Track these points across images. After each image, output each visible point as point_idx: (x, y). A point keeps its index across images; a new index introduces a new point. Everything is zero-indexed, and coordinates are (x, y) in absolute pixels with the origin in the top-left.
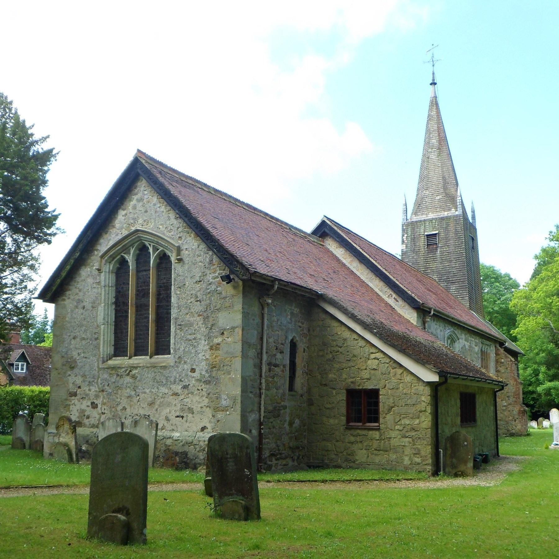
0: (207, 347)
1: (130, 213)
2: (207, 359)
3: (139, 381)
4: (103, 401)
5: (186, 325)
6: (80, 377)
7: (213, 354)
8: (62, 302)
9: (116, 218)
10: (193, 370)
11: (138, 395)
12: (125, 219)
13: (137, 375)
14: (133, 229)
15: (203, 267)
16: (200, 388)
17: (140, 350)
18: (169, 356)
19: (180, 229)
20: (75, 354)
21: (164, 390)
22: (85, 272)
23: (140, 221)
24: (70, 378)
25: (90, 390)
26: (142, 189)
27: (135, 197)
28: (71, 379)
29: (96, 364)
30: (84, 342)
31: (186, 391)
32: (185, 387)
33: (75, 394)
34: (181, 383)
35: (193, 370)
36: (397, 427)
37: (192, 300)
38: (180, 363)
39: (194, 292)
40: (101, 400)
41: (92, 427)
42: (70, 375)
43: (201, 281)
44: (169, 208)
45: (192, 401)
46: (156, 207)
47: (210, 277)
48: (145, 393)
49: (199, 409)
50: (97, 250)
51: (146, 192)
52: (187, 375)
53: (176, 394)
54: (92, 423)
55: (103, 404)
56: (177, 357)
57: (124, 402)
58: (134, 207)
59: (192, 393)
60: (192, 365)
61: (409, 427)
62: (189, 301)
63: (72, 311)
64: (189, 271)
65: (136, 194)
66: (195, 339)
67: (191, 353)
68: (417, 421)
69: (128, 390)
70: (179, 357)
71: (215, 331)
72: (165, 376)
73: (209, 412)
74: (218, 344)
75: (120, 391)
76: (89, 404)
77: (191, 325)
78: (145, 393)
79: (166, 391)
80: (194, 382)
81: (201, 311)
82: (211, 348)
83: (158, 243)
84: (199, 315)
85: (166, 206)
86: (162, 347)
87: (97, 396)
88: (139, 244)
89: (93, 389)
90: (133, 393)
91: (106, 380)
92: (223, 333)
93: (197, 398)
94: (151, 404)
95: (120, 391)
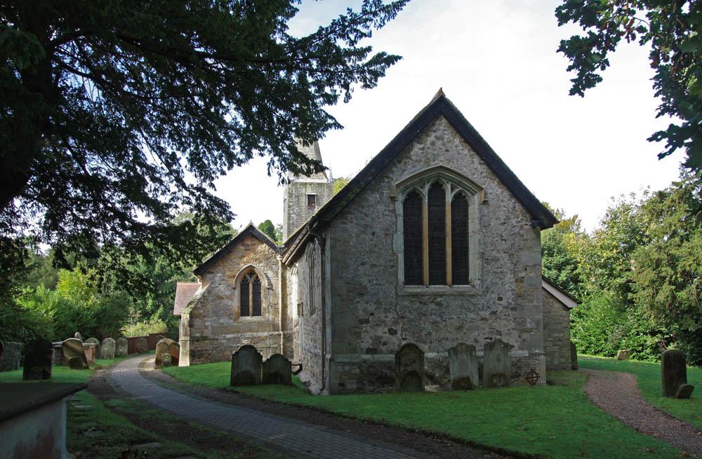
0: (513, 280)
1: (429, 148)
2: (513, 290)
3: (445, 308)
4: (402, 328)
5: (492, 260)
6: (372, 304)
7: (518, 286)
8: (343, 226)
9: (411, 150)
10: (500, 299)
11: (445, 321)
12: (423, 153)
13: (443, 302)
14: (433, 165)
15: (507, 212)
16: (507, 314)
17: (437, 278)
18: (401, 277)
19: (484, 175)
20: (365, 281)
21: (472, 316)
22: (373, 198)
23: (442, 158)
24: (359, 305)
25: (386, 317)
26: (442, 128)
27: (433, 135)
28: (361, 306)
29: (393, 291)
30: (376, 269)
31: (494, 317)
32: (494, 313)
33: (367, 321)
34: (489, 309)
35: (500, 299)
36: (550, 339)
37: (497, 238)
38: (487, 292)
39: (499, 232)
40: (401, 326)
41: (390, 353)
42: (358, 302)
43: (504, 223)
44: (472, 153)
45: (500, 324)
46: (458, 149)
47: (514, 221)
48: (452, 318)
49: (507, 331)
50: (388, 177)
51: (446, 132)
52: (494, 303)
53: (484, 319)
54: (390, 349)
55: (403, 330)
56: (485, 287)
57: (428, 327)
58: (433, 144)
59: (500, 318)
60: (499, 294)
61: (557, 339)
62: (495, 240)
63: (357, 236)
64: (495, 213)
65: (435, 132)
66: (501, 272)
67: (497, 284)
68: (562, 335)
69: (433, 317)
70: (487, 287)
71: (520, 266)
72: (472, 304)
73: (516, 334)
74: (523, 278)
75: (423, 318)
76: (386, 330)
77: (497, 260)
78: (452, 318)
79: (475, 317)
80: (501, 309)
81: (507, 249)
82: (516, 281)
83: (460, 184)
84: (505, 253)
85: (469, 150)
86: (461, 276)
87: (395, 323)
88: (437, 180)
89: (390, 316)
90: (439, 319)
91: (406, 307)
92: (526, 269)
93: (505, 322)
94: (460, 328)
95: (423, 318)
